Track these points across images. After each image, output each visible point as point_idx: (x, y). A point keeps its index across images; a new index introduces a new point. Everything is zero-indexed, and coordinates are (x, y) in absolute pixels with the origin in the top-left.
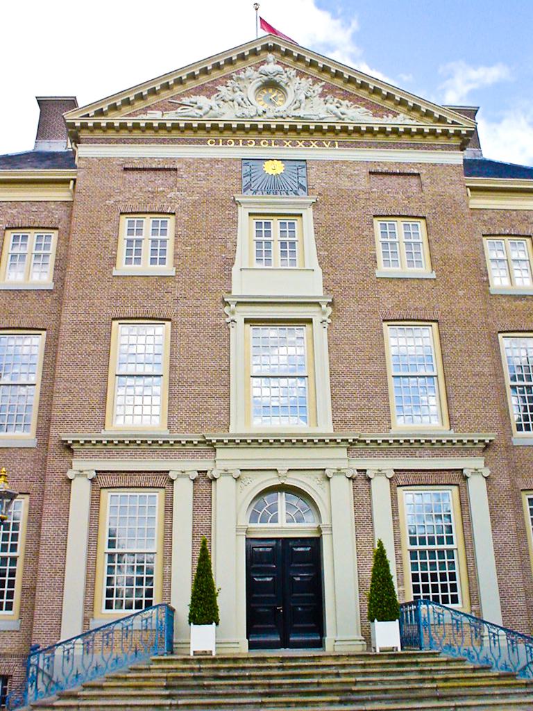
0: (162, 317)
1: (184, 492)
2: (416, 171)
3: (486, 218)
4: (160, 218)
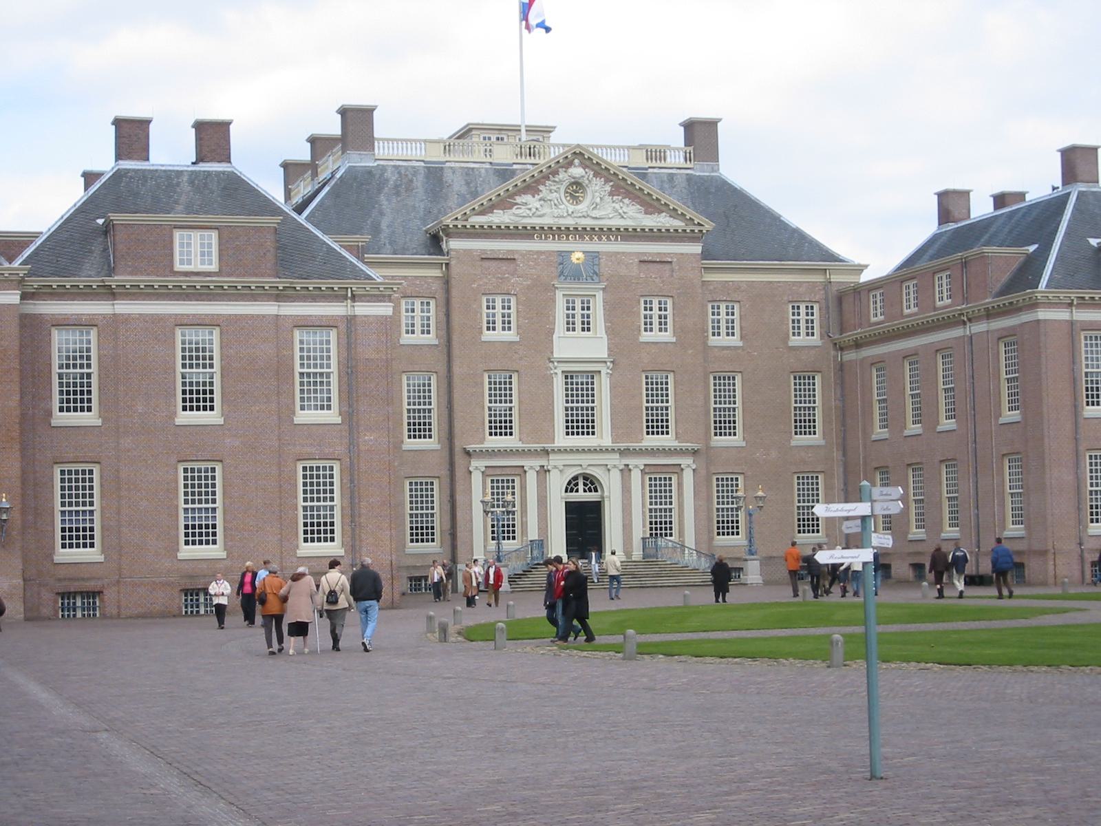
1: (531, 478)
2: (670, 260)
3: (712, 287)
4: (506, 298)
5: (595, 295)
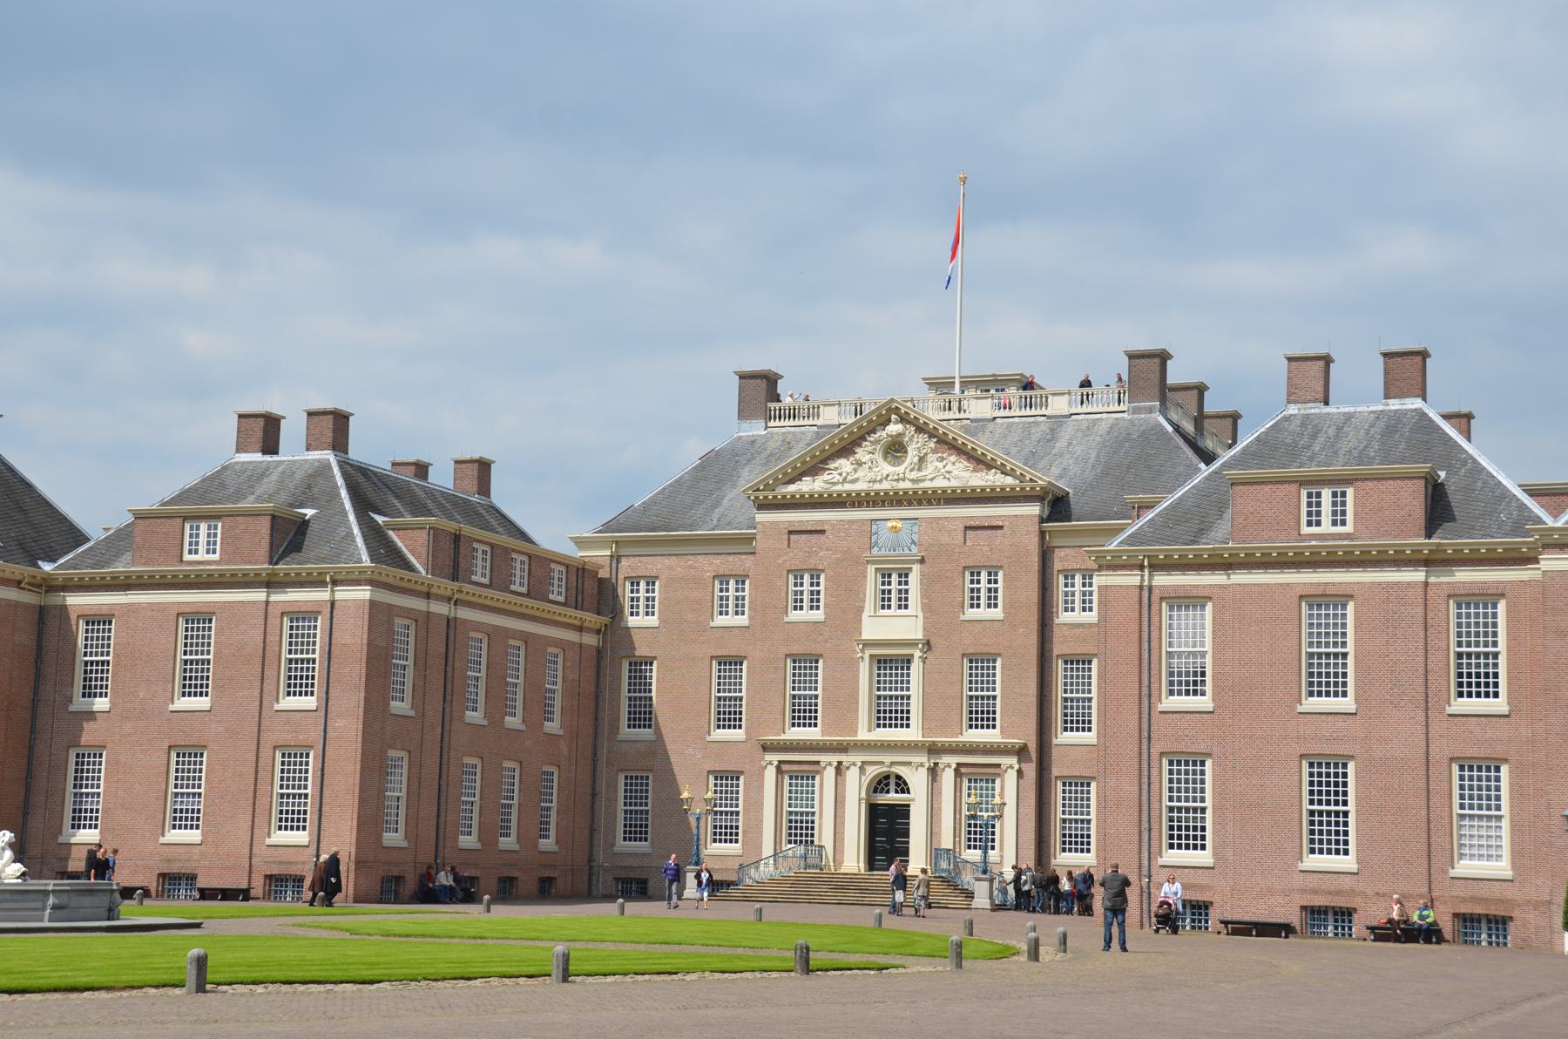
2: (1000, 524)
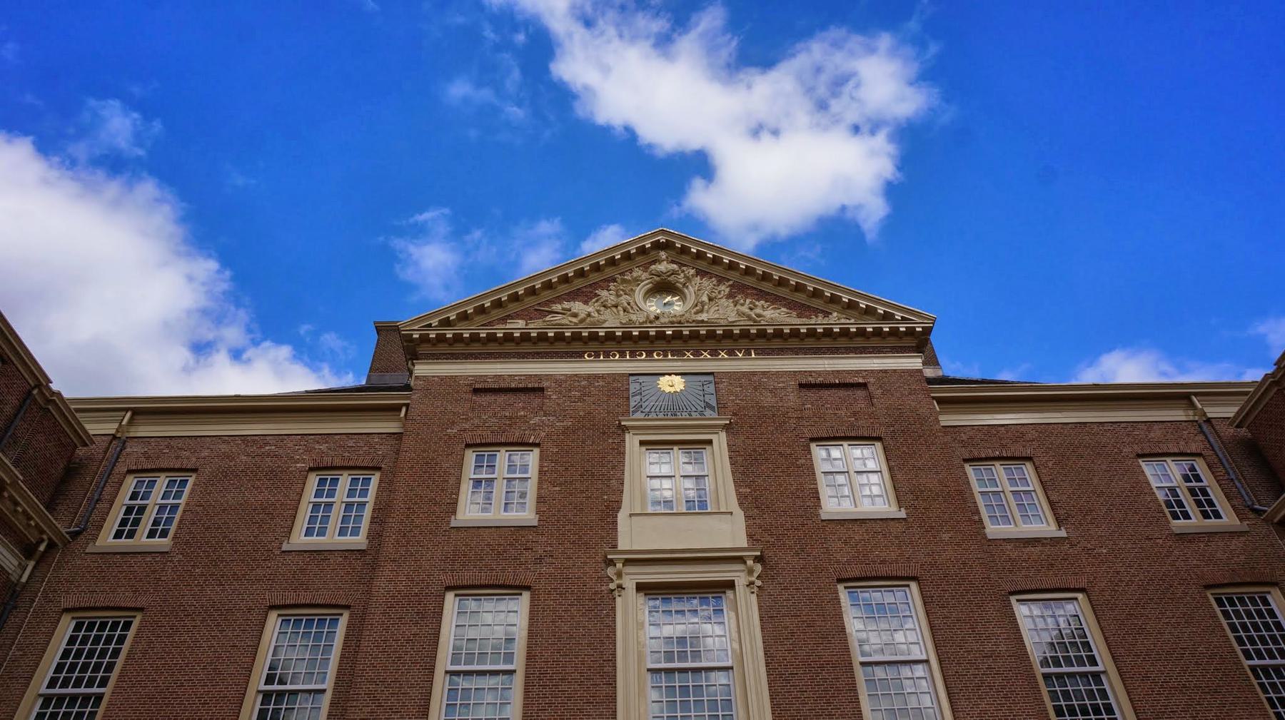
0: (517, 583)
2: (861, 381)
3: (964, 437)
5: (710, 442)
